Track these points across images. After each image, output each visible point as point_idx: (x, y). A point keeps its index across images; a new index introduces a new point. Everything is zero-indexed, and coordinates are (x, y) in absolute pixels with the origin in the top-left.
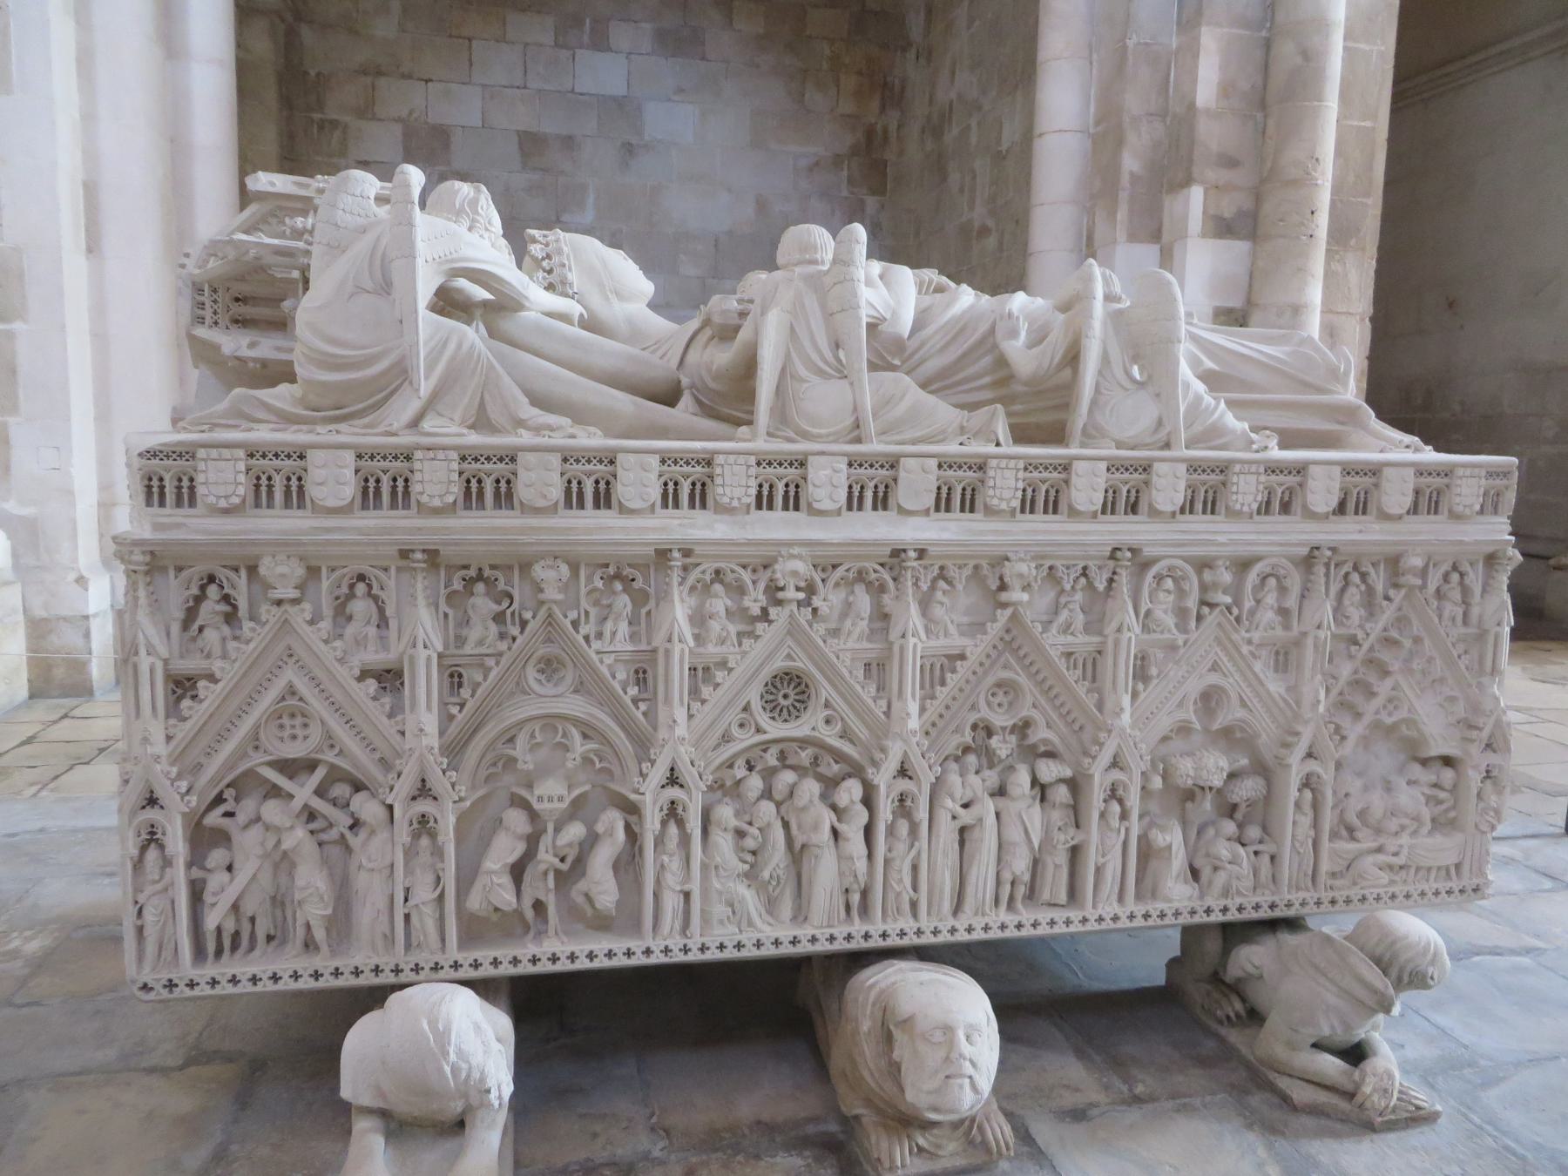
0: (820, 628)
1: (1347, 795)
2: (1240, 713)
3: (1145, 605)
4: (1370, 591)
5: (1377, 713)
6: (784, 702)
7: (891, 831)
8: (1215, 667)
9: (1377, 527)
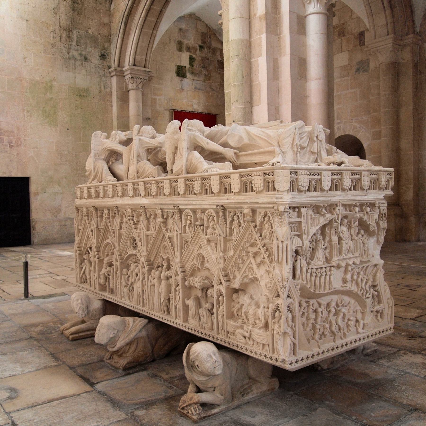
0: (134, 226)
1: (243, 305)
2: (208, 265)
3: (184, 224)
4: (239, 222)
5: (245, 271)
6: (135, 245)
7: (142, 282)
8: (200, 247)
9: (232, 197)
